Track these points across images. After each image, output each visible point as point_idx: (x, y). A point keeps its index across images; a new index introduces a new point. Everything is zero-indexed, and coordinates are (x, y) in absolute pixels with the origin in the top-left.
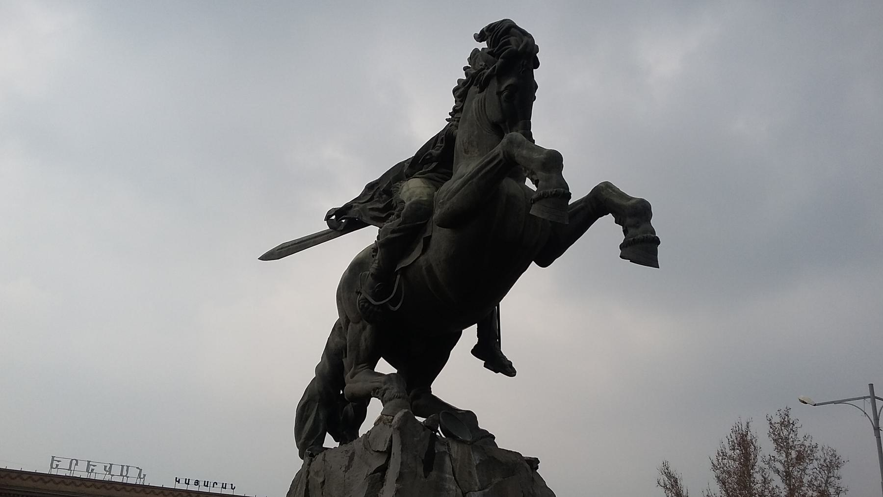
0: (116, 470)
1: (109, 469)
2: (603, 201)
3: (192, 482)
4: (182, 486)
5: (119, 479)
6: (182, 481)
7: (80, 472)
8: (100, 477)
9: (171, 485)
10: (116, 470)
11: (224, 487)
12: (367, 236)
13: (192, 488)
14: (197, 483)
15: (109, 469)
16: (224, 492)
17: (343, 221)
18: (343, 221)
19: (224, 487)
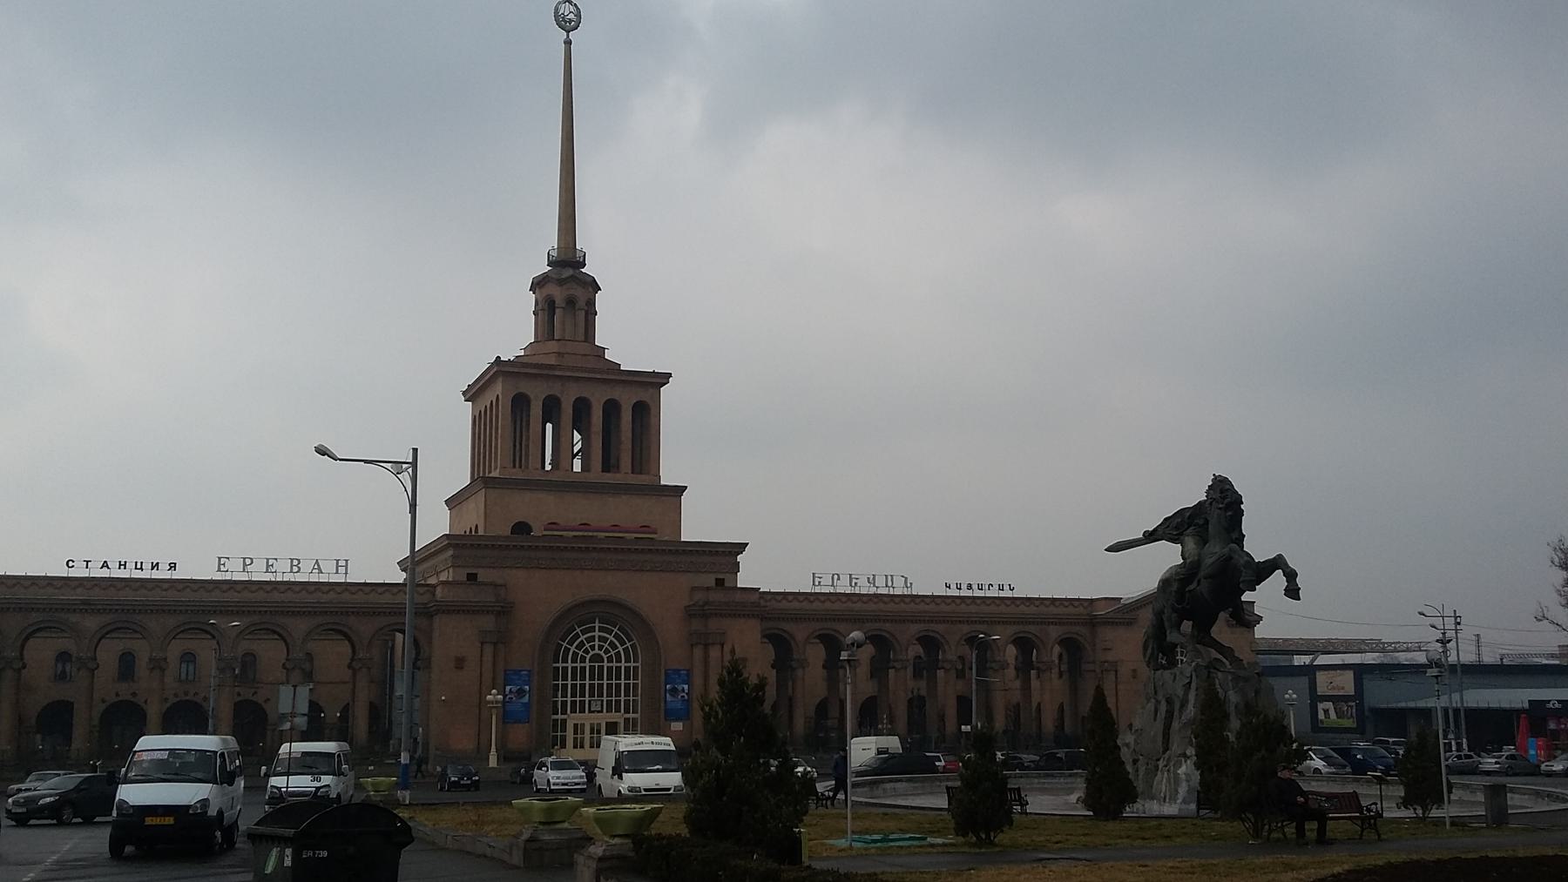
0: (880, 582)
1: (872, 581)
2: (1277, 563)
3: (964, 587)
4: (954, 592)
5: (885, 591)
6: (953, 586)
7: (843, 587)
8: (864, 591)
9: (942, 591)
10: (880, 582)
11: (1001, 588)
12: (1168, 555)
13: (965, 593)
14: (970, 587)
15: (872, 581)
16: (1002, 594)
17: (1151, 537)
18: (1151, 537)
19: (1001, 588)
